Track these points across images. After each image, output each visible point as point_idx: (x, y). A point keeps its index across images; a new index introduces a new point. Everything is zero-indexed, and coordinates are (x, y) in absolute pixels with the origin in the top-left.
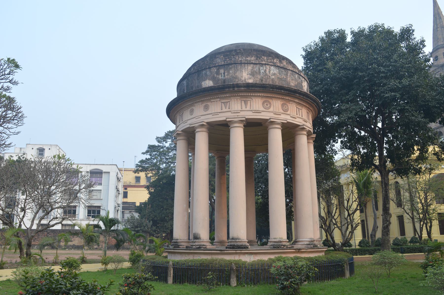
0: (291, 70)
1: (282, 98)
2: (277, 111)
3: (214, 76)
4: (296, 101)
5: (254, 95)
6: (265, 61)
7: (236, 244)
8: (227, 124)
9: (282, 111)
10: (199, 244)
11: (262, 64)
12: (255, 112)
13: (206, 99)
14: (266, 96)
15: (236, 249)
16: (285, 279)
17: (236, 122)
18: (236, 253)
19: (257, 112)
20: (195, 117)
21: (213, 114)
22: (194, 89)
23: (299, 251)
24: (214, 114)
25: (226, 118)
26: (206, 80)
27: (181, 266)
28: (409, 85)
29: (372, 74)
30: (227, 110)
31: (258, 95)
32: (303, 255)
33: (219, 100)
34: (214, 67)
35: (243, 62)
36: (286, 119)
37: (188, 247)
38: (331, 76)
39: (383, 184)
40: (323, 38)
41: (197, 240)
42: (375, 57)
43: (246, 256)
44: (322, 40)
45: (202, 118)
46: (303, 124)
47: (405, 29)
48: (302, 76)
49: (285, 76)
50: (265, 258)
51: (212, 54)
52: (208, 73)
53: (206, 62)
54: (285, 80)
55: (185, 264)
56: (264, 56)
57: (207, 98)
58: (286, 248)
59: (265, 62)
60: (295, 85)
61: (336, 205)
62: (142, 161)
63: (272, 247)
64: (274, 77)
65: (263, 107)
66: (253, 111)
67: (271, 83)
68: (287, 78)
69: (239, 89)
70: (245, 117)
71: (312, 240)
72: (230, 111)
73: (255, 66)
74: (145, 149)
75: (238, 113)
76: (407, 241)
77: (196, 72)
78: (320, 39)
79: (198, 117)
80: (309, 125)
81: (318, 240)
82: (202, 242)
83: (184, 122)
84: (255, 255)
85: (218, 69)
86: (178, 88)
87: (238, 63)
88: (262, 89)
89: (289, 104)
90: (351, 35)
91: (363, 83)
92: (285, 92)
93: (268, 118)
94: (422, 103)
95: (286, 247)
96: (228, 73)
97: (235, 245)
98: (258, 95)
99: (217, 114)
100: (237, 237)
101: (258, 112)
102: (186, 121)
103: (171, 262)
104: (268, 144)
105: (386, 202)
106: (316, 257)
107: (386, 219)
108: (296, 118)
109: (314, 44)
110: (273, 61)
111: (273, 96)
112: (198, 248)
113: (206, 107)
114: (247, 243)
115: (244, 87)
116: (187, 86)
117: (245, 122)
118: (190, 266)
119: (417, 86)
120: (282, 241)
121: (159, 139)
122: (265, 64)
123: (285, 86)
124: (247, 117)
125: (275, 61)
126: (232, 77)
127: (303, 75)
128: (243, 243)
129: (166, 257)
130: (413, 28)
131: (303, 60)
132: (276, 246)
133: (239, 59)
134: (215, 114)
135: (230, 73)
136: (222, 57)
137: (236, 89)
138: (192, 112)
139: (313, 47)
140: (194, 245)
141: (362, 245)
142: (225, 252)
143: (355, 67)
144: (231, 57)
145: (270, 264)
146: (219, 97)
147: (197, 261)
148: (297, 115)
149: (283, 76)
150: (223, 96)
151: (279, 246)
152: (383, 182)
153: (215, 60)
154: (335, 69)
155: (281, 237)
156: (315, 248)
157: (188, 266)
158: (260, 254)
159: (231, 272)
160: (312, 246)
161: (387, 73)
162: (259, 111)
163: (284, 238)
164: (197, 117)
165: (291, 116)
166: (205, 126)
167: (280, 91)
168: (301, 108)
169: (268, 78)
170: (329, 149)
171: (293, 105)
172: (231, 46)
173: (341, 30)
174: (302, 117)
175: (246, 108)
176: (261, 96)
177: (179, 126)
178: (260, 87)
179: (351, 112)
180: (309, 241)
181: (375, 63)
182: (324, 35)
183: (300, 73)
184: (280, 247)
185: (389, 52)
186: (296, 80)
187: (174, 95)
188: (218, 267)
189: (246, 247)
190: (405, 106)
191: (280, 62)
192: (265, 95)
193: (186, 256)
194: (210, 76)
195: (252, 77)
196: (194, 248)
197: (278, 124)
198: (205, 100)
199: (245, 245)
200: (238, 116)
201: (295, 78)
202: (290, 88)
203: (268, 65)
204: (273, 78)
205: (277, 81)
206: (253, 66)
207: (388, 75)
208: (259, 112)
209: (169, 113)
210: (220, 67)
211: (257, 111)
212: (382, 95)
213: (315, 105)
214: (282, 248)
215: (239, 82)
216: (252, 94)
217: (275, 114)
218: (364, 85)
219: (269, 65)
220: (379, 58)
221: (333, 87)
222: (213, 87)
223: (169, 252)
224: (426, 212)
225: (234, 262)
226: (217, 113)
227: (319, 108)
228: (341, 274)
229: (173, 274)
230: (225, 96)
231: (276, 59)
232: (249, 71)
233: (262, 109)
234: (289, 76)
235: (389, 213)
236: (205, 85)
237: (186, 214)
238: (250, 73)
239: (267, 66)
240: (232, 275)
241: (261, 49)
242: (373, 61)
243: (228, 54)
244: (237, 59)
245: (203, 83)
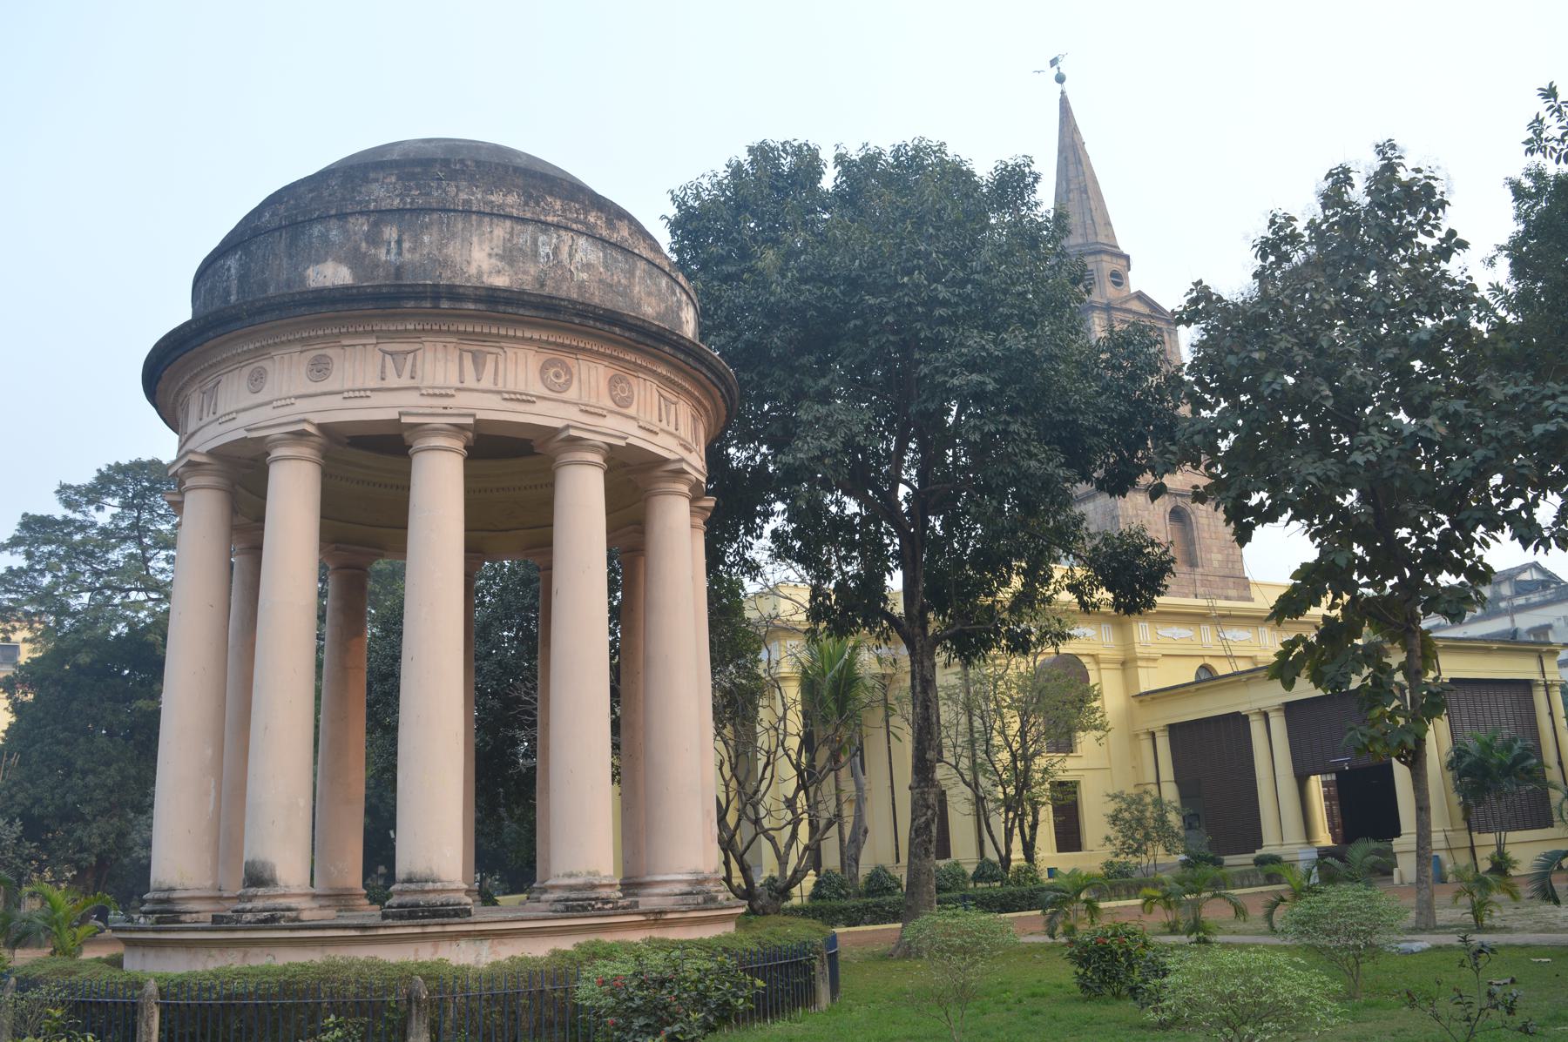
0: (646, 259)
1: (611, 356)
2: (593, 401)
3: (357, 249)
4: (659, 370)
5: (511, 333)
6: (559, 216)
7: (421, 899)
8: (400, 436)
9: (610, 404)
10: (270, 903)
12: (512, 400)
13: (320, 333)
14: (555, 343)
15: (426, 921)
16: (647, 1025)
17: (436, 431)
18: (424, 937)
19: (518, 400)
20: (271, 402)
21: (346, 395)
22: (272, 291)
23: (657, 918)
24: (351, 394)
25: (400, 414)
26: (326, 260)
27: (198, 997)
28: (1028, 351)
29: (909, 305)
30: (405, 381)
31: (528, 334)
32: (674, 934)
33: (374, 341)
34: (361, 213)
35: (474, 209)
37: (222, 917)
38: (772, 299)
39: (918, 682)
40: (740, 165)
41: (261, 891)
42: (922, 248)
43: (463, 944)
44: (736, 171)
45: (302, 406)
46: (677, 457)
47: (1009, 168)
48: (681, 286)
50: (539, 949)
51: (351, 167)
52: (334, 234)
53: (326, 194)
54: (626, 293)
55: (214, 987)
56: (551, 194)
57: (327, 332)
58: (612, 909)
59: (556, 219)
60: (658, 314)
61: (767, 752)
63: (560, 906)
64: (585, 276)
65: (542, 379)
66: (507, 396)
68: (630, 285)
69: (458, 305)
70: (473, 415)
71: (700, 877)
72: (417, 388)
73: (518, 228)
75: (447, 395)
76: (964, 874)
77: (285, 227)
78: (730, 170)
79: (283, 402)
80: (696, 463)
82: (284, 896)
83: (224, 419)
84: (496, 941)
85: (376, 225)
86: (200, 284)
87: (455, 211)
88: (543, 315)
89: (633, 381)
90: (835, 167)
91: (876, 333)
92: (627, 334)
93: (558, 424)
94: (1057, 417)
95: (611, 905)
96: (416, 241)
97: (418, 906)
98: (528, 334)
99: (362, 393)
100: (428, 871)
101: (526, 399)
102: (231, 417)
103: (152, 981)
104: (552, 525)
105: (927, 744)
106: (718, 938)
107: (925, 800)
109: (713, 186)
110: (586, 218)
111: (582, 345)
112: (265, 921)
113: (320, 367)
114: (462, 895)
115: (477, 300)
116: (243, 278)
117: (470, 435)
118: (238, 996)
119: (1052, 358)
120: (597, 882)
121: (68, 495)
122: (558, 226)
123: (626, 312)
124: (481, 415)
125: (592, 220)
126: (429, 258)
127: (683, 283)
128: (452, 894)
129: (116, 962)
130: (1034, 168)
131: (669, 236)
132: (575, 903)
133: (461, 194)
134: (357, 394)
135: (422, 242)
136: (393, 179)
137: (445, 304)
138: (258, 380)
139: (707, 193)
140: (250, 911)
141: (824, 892)
142: (381, 932)
143: (854, 274)
144: (429, 186)
145: (562, 973)
146: (373, 331)
147: (266, 972)
148: (660, 421)
149: (619, 278)
150: (393, 328)
152: (918, 676)
153: (363, 190)
154: (784, 276)
155: (592, 869)
156: (713, 906)
157: (229, 997)
158: (515, 934)
159: (410, 1010)
160: (700, 899)
161: (957, 304)
162: (527, 395)
163: (604, 873)
164: (279, 403)
165: (641, 424)
166: (312, 438)
167: (606, 327)
168: (674, 399)
169: (564, 279)
170: (732, 559)
171: (648, 383)
172: (427, 145)
173: (806, 145)
174: (677, 433)
175: (479, 380)
176: (535, 341)
177: (199, 434)
178: (536, 307)
179: (832, 434)
180: (689, 882)
181: (919, 268)
182: (744, 157)
183: (674, 275)
184: (590, 905)
185: (965, 238)
186: (661, 297)
187: (181, 312)
188: (356, 995)
189: (461, 912)
190: (1007, 423)
191: (610, 225)
192: (553, 340)
193: (210, 956)
194: (341, 248)
195: (507, 268)
196: (249, 922)
197: (594, 448)
198: (318, 337)
199: (459, 904)
200: (446, 408)
201: (660, 291)
202: (644, 321)
203: (567, 229)
204: (583, 281)
205: (597, 293)
206: (513, 229)
207: (961, 312)
208: (529, 401)
209: (157, 383)
210: (382, 216)
211: (519, 396)
212: (939, 378)
213: (719, 394)
214: (599, 909)
215: (457, 282)
216: (503, 332)
217: (586, 412)
218: (879, 341)
219: (572, 230)
220: (934, 255)
221: (776, 340)
222: (355, 291)
223: (131, 944)
224: (1023, 781)
225: (424, 972)
226: (364, 393)
227: (732, 405)
228: (804, 996)
229: (160, 1030)
230: (399, 328)
231: (594, 214)
232: (495, 242)
233: (538, 388)
234: (637, 280)
235: (933, 780)
236: (321, 278)
237: (213, 784)
238: (501, 252)
239: (563, 233)
240: (414, 1017)
241: (538, 169)
242: (915, 262)
243: (418, 174)
244: (453, 194)
245: (311, 272)
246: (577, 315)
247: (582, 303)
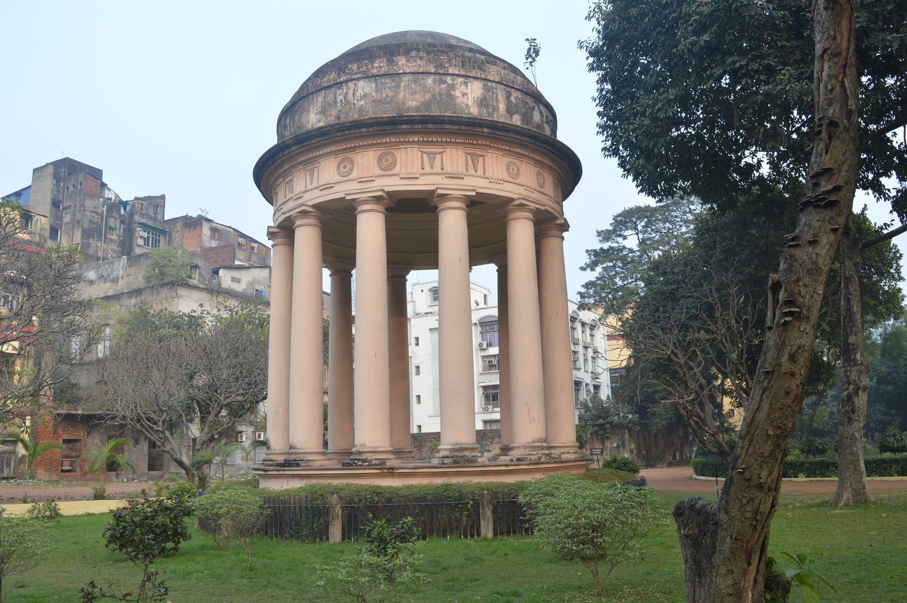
2: (366, 174)
9: (379, 172)
11: (341, 83)
31: (325, 151)
36: (381, 188)
49: (392, 91)
62: (588, 285)
64: (363, 103)
65: (338, 172)
66: (321, 188)
67: (356, 117)
71: (456, 447)
74: (585, 259)
81: (532, 445)
87: (304, 97)
88: (322, 139)
101: (328, 187)
105: (849, 330)
107: (847, 377)
108: (418, 178)
115: (295, 144)
121: (605, 235)
122: (346, 81)
151: (351, 462)
160: (451, 460)
165: (402, 176)
167: (357, 131)
168: (440, 150)
169: (350, 109)
171: (409, 149)
202: (376, 118)
203: (351, 80)
204: (362, 106)
205: (370, 109)
208: (330, 187)
214: (360, 465)
217: (361, 182)
219: (355, 79)
239: (350, 83)
246: (338, 131)
247: (336, 124)
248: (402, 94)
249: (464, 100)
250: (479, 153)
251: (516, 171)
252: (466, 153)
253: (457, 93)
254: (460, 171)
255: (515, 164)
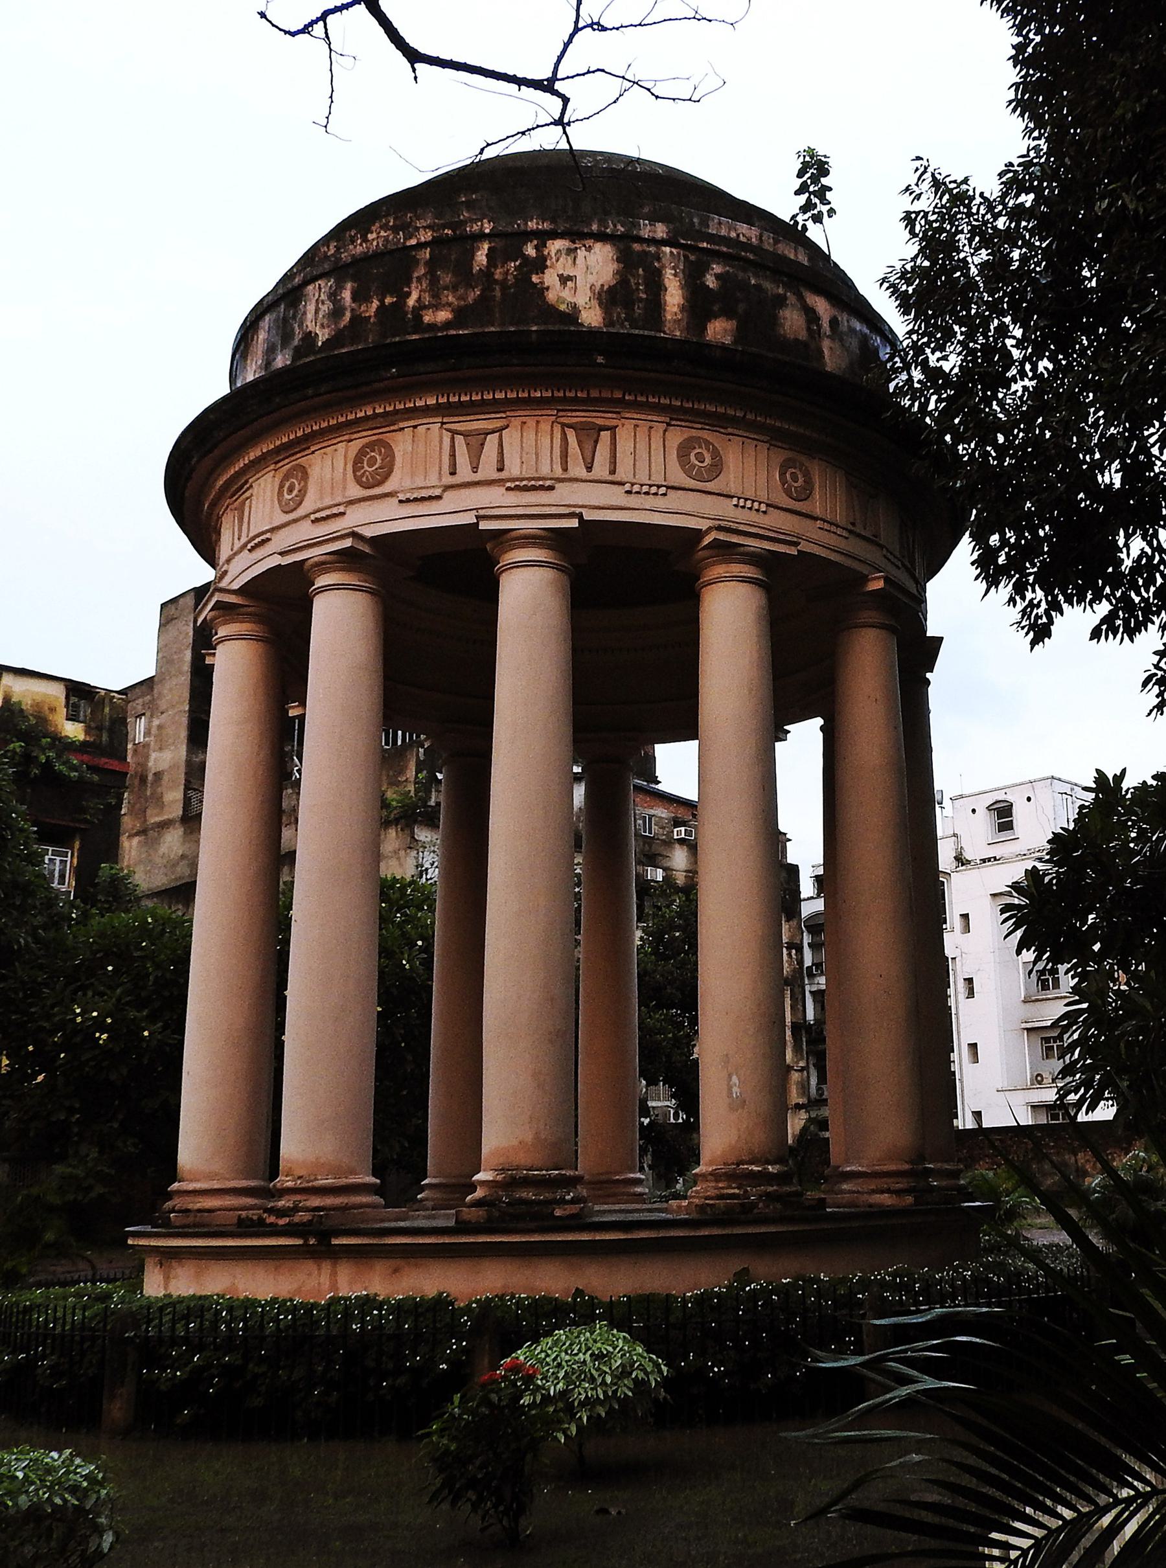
108: (439, 498)
165: (402, 497)
248: (414, 296)
249: (566, 294)
250: (599, 422)
251: (708, 461)
252: (563, 425)
253: (550, 278)
254: (545, 470)
255: (707, 443)
